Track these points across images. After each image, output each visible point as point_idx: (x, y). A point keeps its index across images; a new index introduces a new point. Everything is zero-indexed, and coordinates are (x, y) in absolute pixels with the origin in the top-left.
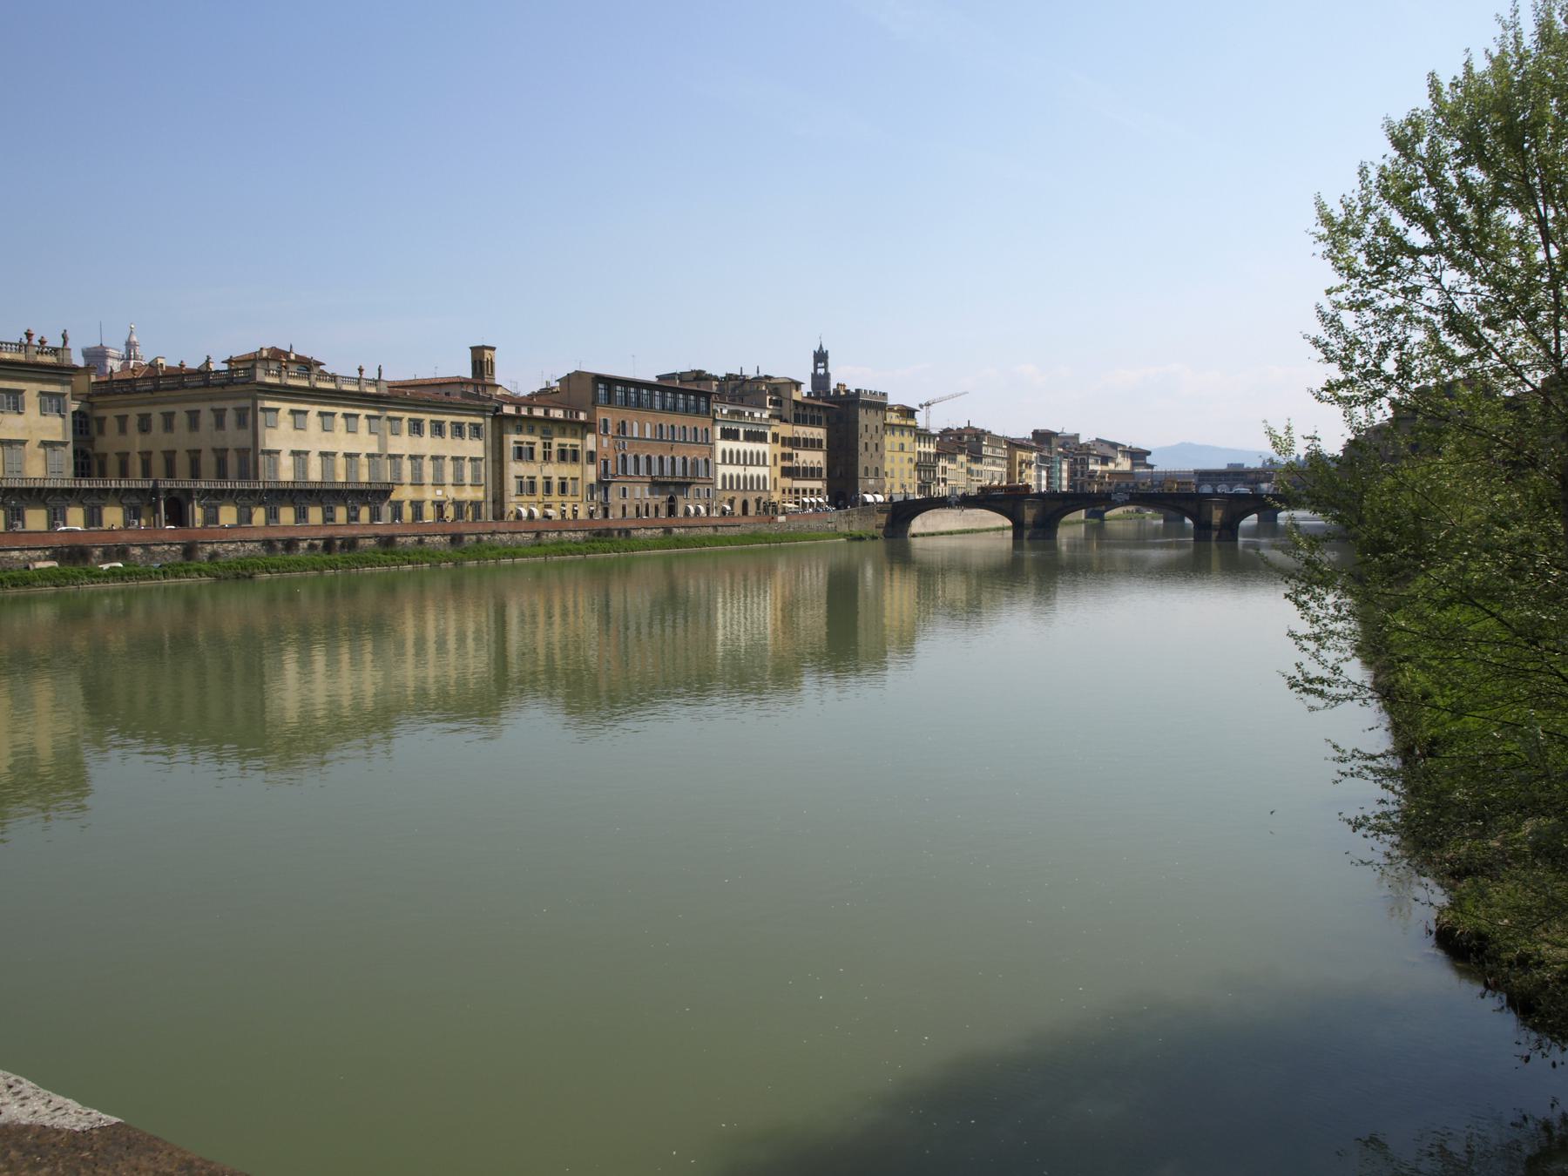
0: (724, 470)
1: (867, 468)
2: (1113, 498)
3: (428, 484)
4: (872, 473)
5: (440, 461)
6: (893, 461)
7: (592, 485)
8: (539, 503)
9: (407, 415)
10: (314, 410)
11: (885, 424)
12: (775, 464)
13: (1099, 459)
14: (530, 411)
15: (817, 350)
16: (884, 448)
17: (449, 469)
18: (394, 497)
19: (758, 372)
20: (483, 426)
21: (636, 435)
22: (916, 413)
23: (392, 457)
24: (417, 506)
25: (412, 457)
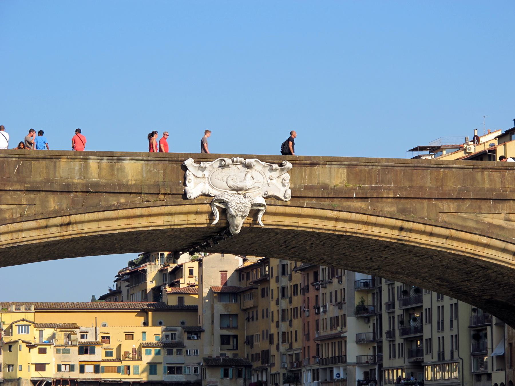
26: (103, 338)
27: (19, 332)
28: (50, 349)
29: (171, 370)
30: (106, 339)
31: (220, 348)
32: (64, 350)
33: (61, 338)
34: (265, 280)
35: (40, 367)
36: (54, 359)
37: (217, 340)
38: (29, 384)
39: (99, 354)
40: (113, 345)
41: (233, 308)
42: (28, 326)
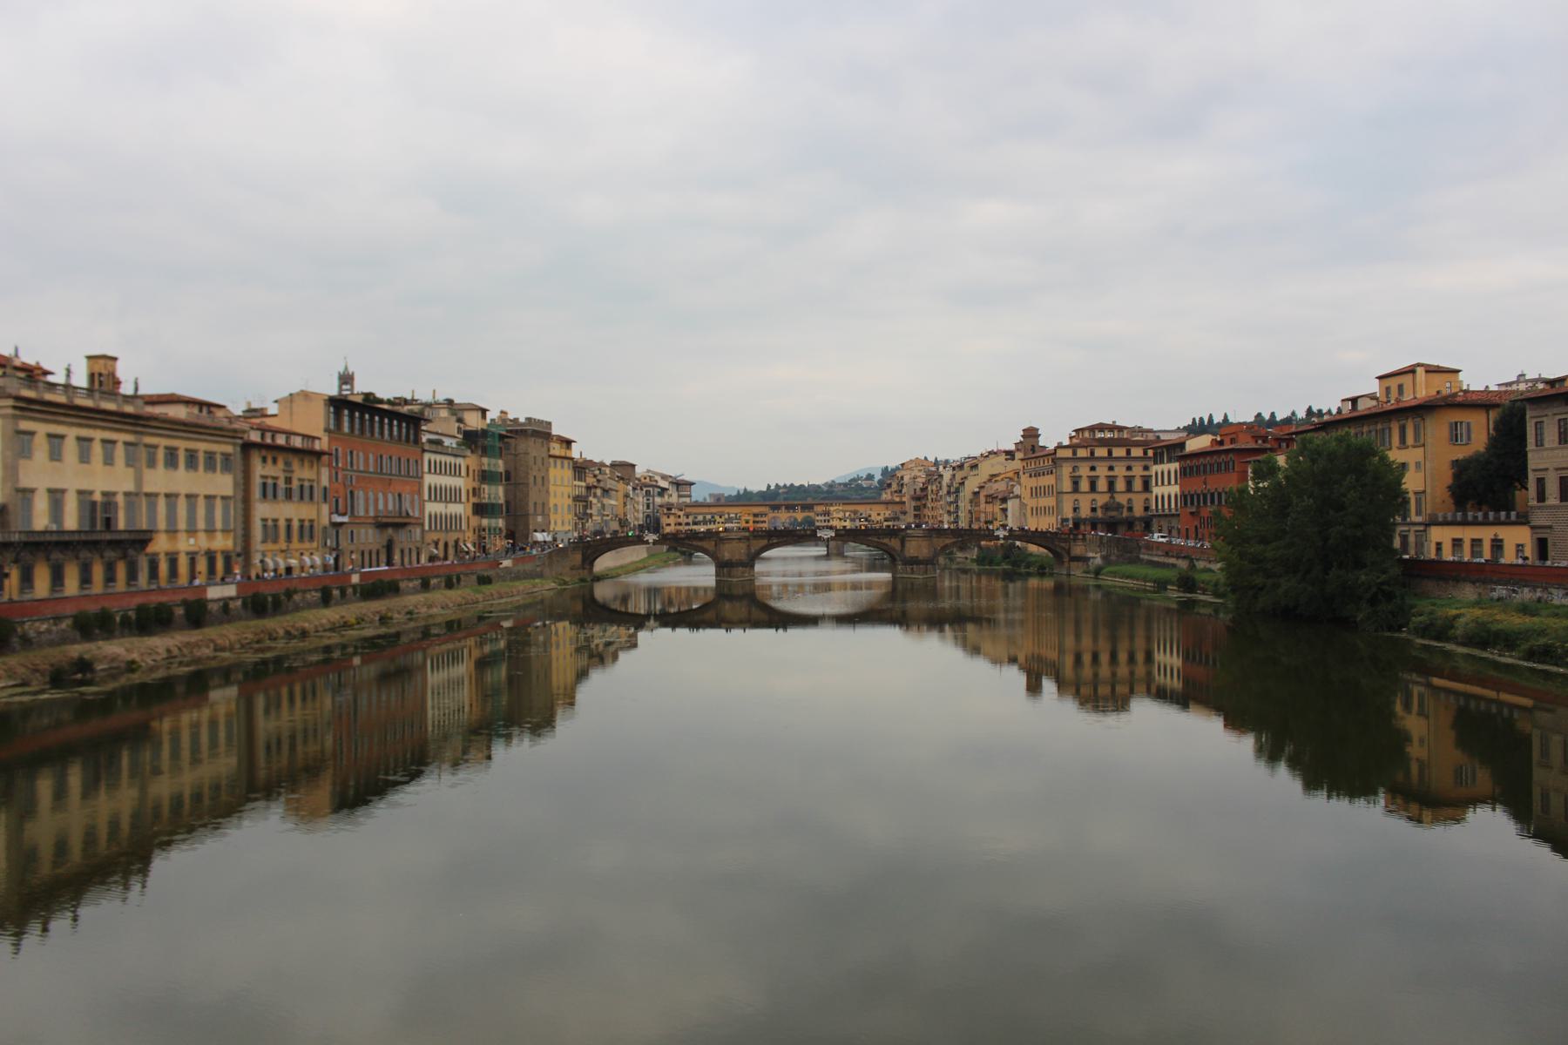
0: (433, 508)
1: (535, 504)
2: (818, 535)
3: (201, 531)
4: (539, 510)
5: (174, 498)
6: (555, 496)
7: (325, 528)
8: (282, 551)
9: (164, 442)
10: (72, 433)
11: (550, 456)
12: (468, 500)
13: (659, 490)
14: (273, 438)
16: (549, 482)
17: (182, 507)
18: (151, 549)
19: (434, 397)
20: (232, 458)
21: (362, 468)
22: (573, 444)
23: (148, 495)
24: (173, 560)
25: (167, 496)
28: (848, 520)
30: (870, 516)
32: (853, 520)
33: (852, 516)
34: (927, 495)
37: (912, 516)
40: (873, 518)
41: (918, 503)
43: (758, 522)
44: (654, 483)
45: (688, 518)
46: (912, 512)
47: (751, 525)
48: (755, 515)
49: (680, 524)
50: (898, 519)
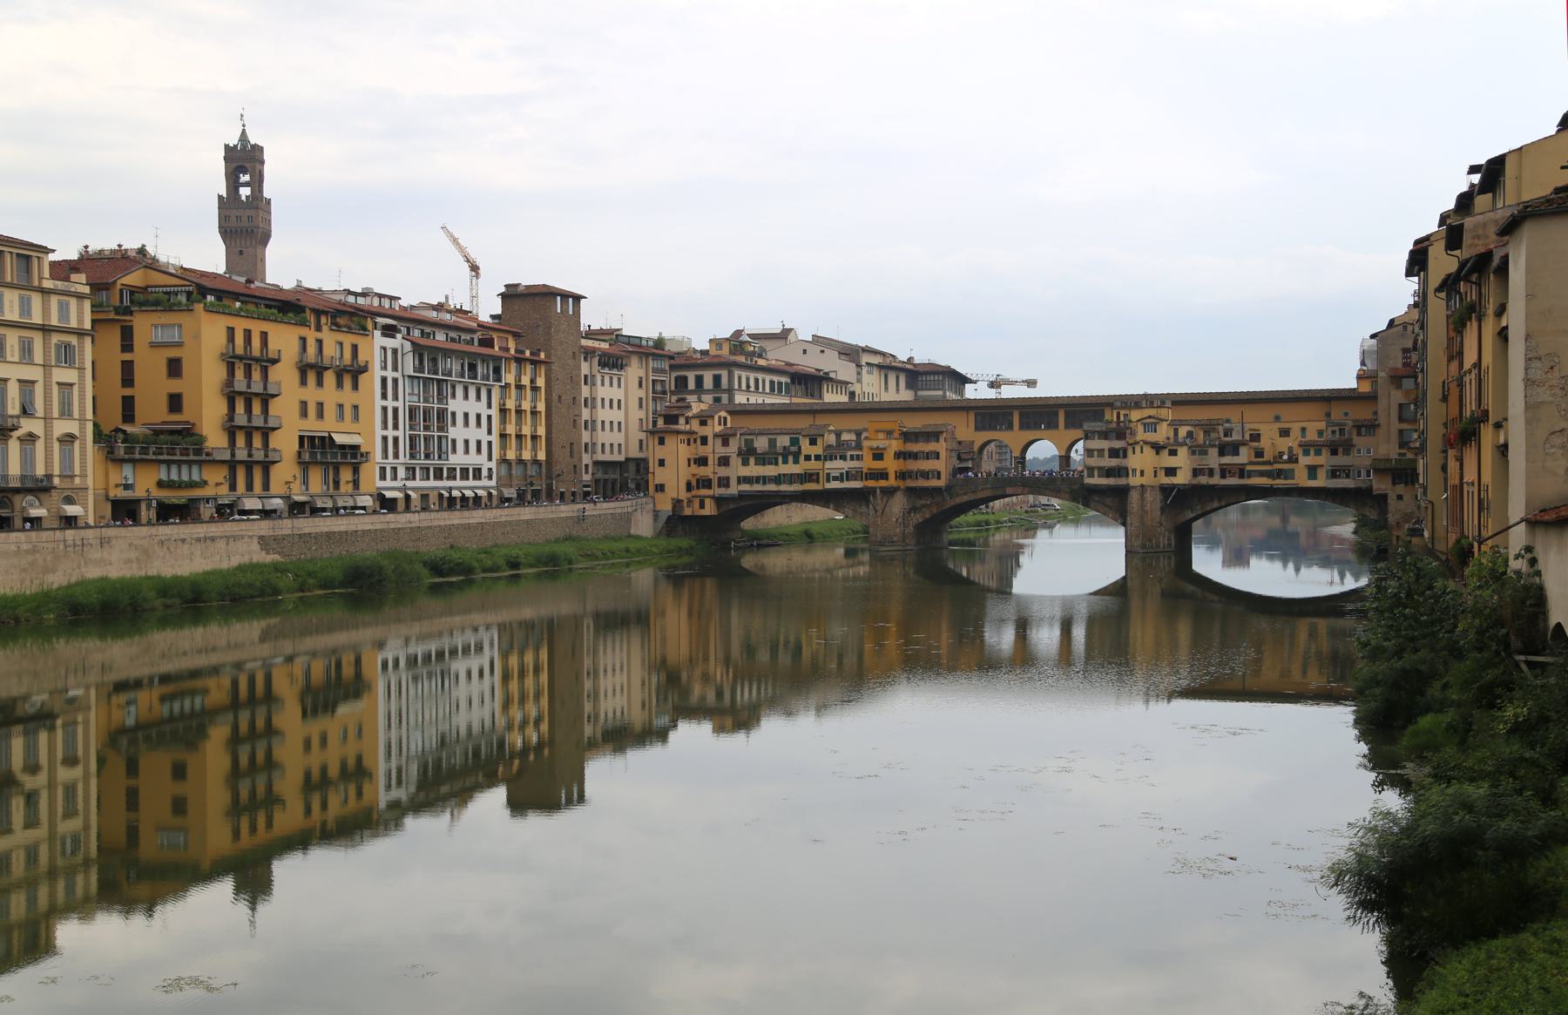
13: (784, 380)
15: (233, 140)
26: (1251, 435)
27: (1145, 432)
28: (1183, 452)
29: (1334, 474)
30: (1256, 437)
31: (1397, 447)
32: (1198, 450)
33: (1200, 437)
35: (1171, 472)
36: (1189, 462)
38: (1158, 492)
39: (1244, 456)
42: (1155, 424)
43: (914, 456)
44: (742, 359)
45: (725, 443)
46: (1390, 422)
47: (890, 464)
48: (907, 436)
49: (702, 461)
50: (1348, 447)
